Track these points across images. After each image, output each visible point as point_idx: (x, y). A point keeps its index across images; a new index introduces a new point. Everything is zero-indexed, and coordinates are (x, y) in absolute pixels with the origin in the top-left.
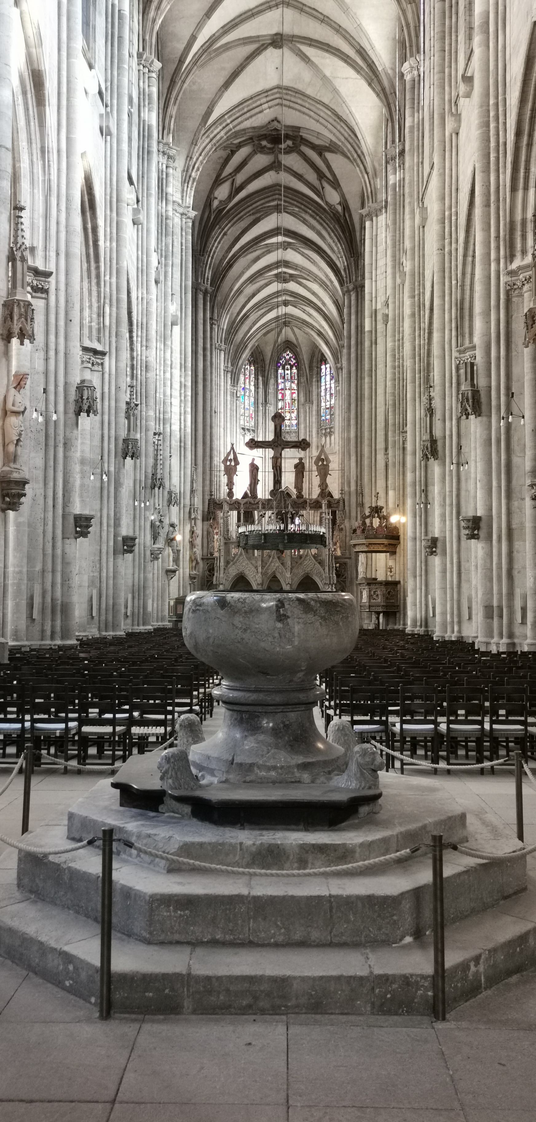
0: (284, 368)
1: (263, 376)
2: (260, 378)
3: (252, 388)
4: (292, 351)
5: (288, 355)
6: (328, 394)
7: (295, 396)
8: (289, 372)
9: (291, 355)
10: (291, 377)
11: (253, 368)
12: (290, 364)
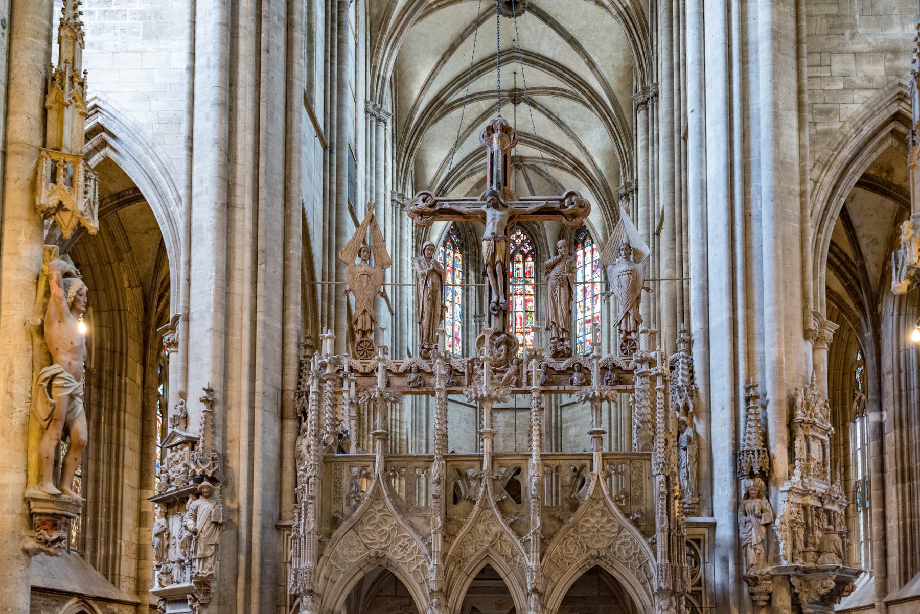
1: (477, 270)
2: (472, 274)
3: (458, 290)
4: (525, 230)
5: (518, 237)
6: (589, 296)
7: (531, 305)
8: (520, 265)
9: (524, 237)
10: (525, 274)
11: (458, 255)
12: (522, 252)
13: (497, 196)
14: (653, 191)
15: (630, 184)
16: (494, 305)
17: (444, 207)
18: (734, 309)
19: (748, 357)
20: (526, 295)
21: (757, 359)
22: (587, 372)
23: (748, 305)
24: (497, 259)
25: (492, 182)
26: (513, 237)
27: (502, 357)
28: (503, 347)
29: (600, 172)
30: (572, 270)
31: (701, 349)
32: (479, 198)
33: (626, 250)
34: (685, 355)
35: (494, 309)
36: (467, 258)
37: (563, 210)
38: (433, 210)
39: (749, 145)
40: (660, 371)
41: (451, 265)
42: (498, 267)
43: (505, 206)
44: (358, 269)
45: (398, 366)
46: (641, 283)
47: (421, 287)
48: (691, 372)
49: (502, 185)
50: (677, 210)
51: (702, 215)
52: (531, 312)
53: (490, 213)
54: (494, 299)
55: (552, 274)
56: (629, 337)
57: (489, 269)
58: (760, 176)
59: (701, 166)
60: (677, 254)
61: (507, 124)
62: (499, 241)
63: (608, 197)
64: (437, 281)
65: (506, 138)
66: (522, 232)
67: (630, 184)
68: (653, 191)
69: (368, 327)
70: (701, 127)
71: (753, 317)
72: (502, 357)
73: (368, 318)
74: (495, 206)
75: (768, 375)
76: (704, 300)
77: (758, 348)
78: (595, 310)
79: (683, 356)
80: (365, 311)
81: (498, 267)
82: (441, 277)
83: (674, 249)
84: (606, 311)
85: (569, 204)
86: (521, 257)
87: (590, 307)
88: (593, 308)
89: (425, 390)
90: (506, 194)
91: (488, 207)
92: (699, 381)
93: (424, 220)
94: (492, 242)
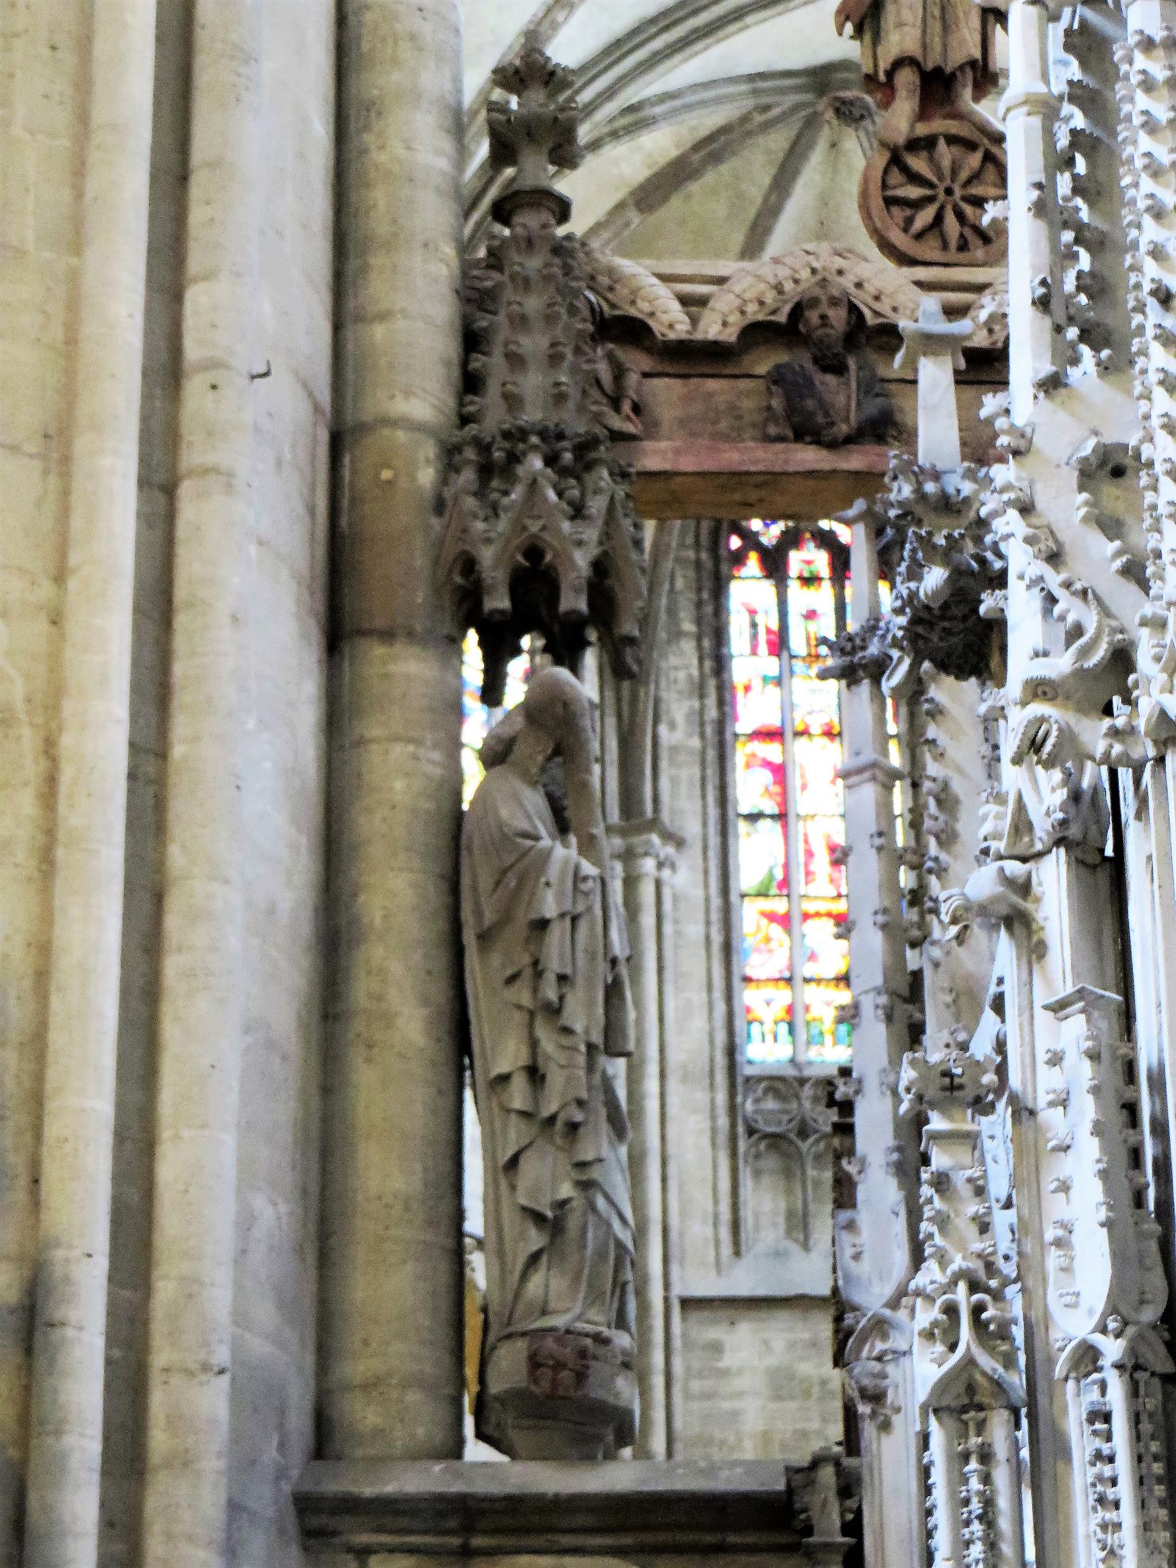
0: (774, 564)
86: (820, 560)
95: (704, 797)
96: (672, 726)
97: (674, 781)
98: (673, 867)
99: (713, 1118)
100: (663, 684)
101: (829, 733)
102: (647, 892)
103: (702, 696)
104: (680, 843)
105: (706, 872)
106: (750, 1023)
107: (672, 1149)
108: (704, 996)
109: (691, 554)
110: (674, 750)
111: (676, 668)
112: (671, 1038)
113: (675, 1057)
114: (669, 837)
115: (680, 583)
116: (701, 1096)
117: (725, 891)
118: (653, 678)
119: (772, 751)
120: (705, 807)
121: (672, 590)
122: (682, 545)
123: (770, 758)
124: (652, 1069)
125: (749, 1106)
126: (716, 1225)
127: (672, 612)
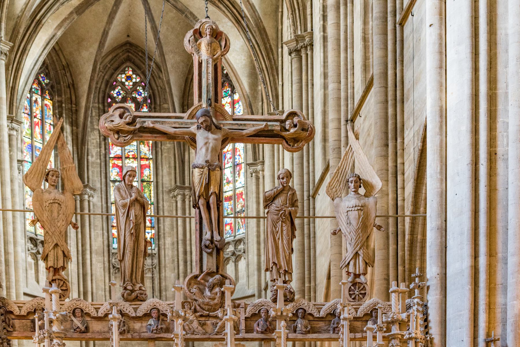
1: (74, 123)
4: (139, 69)
9: (136, 79)
11: (48, 102)
12: (134, 100)
13: (210, 117)
14: (346, 65)
15: (303, 38)
16: (208, 243)
17: (146, 125)
18: (476, 256)
19: (490, 308)
20: (142, 159)
21: (498, 311)
22: (311, 318)
23: (491, 254)
24: (211, 190)
25: (200, 96)
26: (122, 78)
27: (216, 301)
28: (217, 290)
29: (252, 6)
30: (293, 204)
31: (438, 297)
32: (186, 115)
33: (356, 182)
34: (421, 303)
35: (207, 247)
36: (60, 106)
37: (284, 134)
38: (132, 128)
39: (496, 75)
40: (413, 335)
41: (39, 116)
42: (212, 200)
43: (218, 128)
44: (46, 196)
45: (97, 309)
46: (372, 221)
47: (123, 220)
48: (426, 320)
49: (213, 101)
50: (390, 111)
51: (441, 147)
52: (149, 182)
53: (201, 136)
54: (207, 236)
55: (273, 207)
56: (358, 280)
57: (201, 202)
58: (507, 111)
59: (441, 91)
60: (391, 164)
61: (217, 26)
62: (214, 170)
63: (263, 39)
64: (140, 213)
65: (216, 44)
66: (134, 71)
67: (303, 38)
68: (346, 65)
69: (61, 264)
70: (441, 44)
71: (495, 266)
72: (216, 301)
73: (60, 253)
74: (208, 129)
75: (509, 328)
76: (441, 242)
77: (499, 299)
78: (238, 185)
79: (418, 304)
80: (56, 245)
81: (212, 200)
82: (143, 207)
83: (386, 157)
84: (254, 188)
85: (291, 127)
87: (231, 179)
88: (235, 181)
89: (129, 336)
90: (220, 113)
91: (199, 128)
92: (435, 330)
93: (121, 140)
94: (206, 170)
95: (101, 177)
96: (92, 156)
97: (93, 172)
98: (93, 197)
99: (104, 264)
100: (90, 144)
101: (134, 158)
102: (86, 204)
103: (100, 148)
104: (94, 190)
105: (102, 198)
106: (113, 238)
107: (94, 272)
108: (101, 232)
109: (97, 105)
110: (93, 163)
111: (93, 139)
112: (93, 243)
113: (94, 248)
114: (91, 189)
115: (94, 114)
116: (101, 258)
117: (107, 203)
118: (86, 144)
119: (119, 163)
120: (101, 180)
121: (91, 116)
122: (94, 102)
123: (119, 164)
124: (88, 252)
125: (113, 260)
126: (105, 292)
127: (92, 123)
